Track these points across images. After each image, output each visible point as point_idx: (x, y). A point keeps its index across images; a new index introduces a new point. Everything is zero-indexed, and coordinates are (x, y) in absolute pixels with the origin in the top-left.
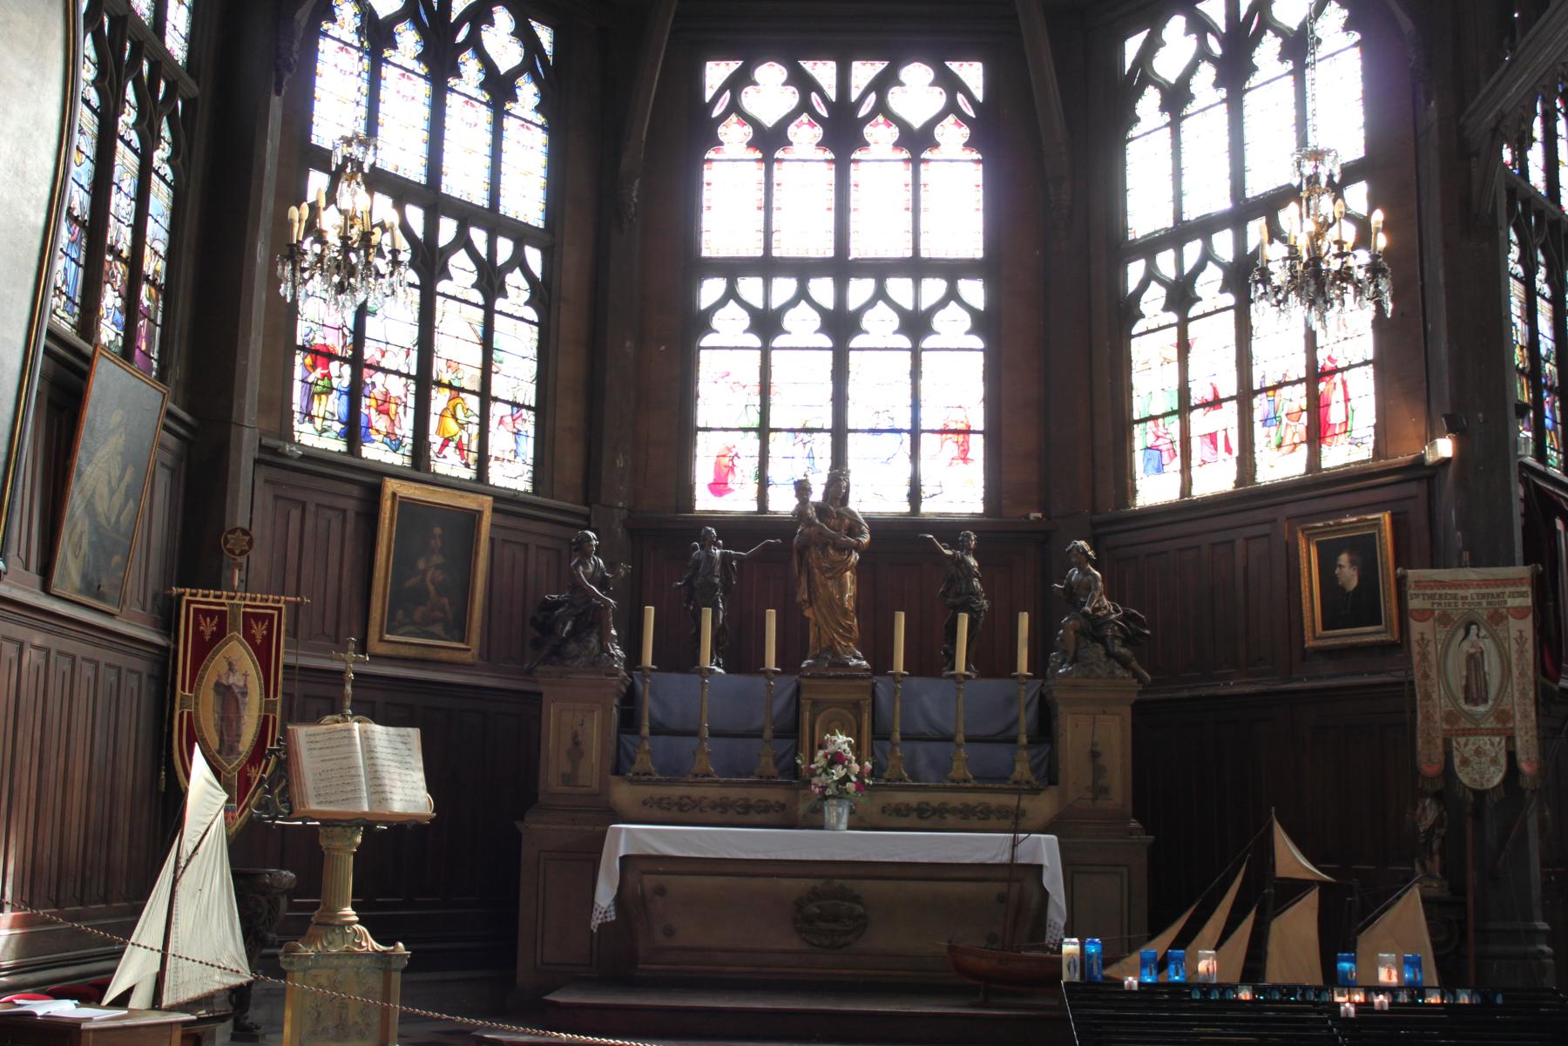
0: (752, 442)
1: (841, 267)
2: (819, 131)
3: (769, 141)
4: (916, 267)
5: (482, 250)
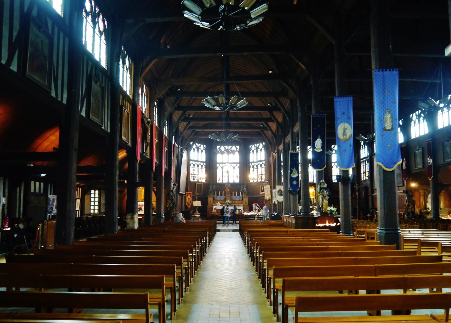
4: (234, 163)
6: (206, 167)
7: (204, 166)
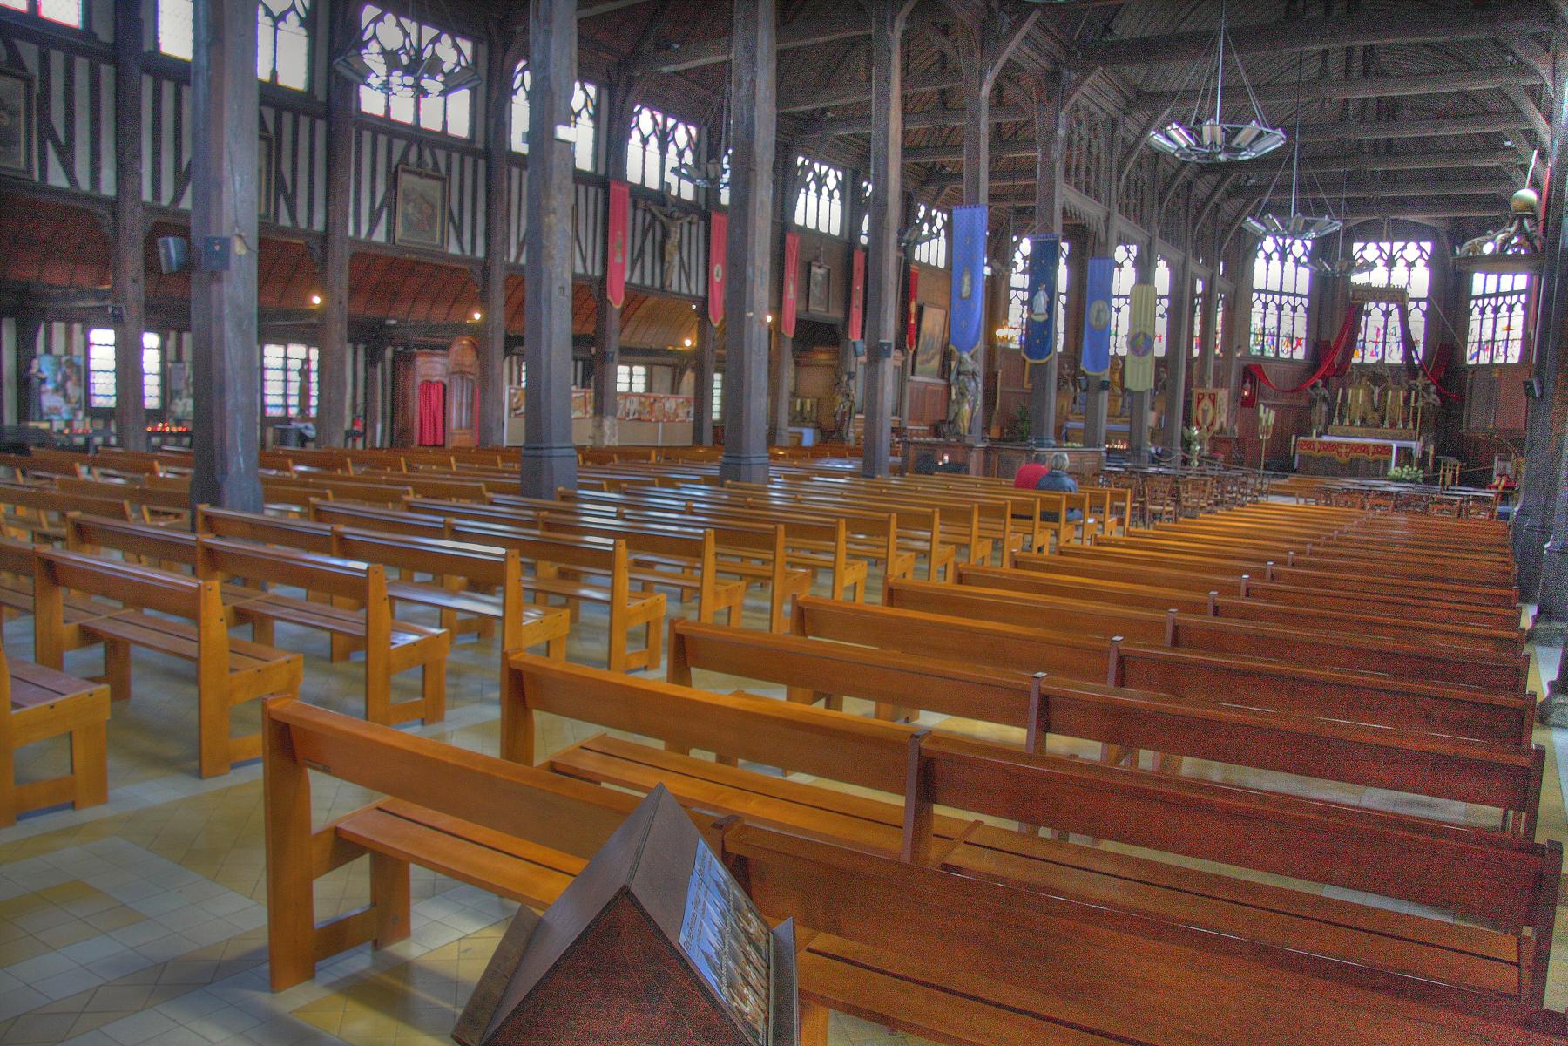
6: (1307, 310)
7: (1301, 310)
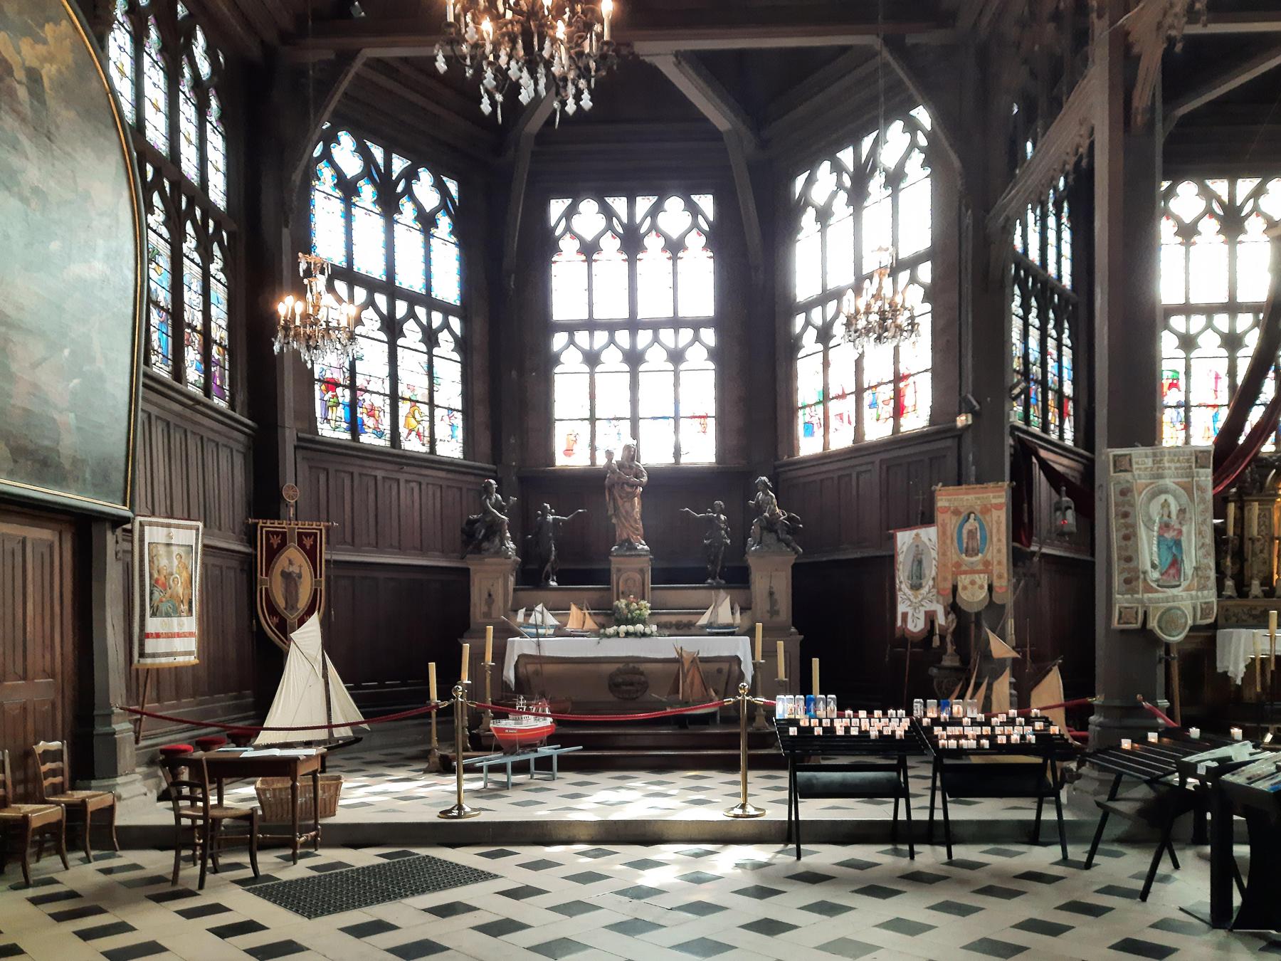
0: (587, 424)
1: (633, 325)
2: (618, 242)
3: (589, 250)
4: (676, 323)
5: (424, 321)
